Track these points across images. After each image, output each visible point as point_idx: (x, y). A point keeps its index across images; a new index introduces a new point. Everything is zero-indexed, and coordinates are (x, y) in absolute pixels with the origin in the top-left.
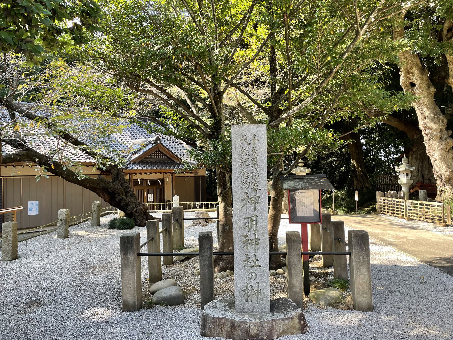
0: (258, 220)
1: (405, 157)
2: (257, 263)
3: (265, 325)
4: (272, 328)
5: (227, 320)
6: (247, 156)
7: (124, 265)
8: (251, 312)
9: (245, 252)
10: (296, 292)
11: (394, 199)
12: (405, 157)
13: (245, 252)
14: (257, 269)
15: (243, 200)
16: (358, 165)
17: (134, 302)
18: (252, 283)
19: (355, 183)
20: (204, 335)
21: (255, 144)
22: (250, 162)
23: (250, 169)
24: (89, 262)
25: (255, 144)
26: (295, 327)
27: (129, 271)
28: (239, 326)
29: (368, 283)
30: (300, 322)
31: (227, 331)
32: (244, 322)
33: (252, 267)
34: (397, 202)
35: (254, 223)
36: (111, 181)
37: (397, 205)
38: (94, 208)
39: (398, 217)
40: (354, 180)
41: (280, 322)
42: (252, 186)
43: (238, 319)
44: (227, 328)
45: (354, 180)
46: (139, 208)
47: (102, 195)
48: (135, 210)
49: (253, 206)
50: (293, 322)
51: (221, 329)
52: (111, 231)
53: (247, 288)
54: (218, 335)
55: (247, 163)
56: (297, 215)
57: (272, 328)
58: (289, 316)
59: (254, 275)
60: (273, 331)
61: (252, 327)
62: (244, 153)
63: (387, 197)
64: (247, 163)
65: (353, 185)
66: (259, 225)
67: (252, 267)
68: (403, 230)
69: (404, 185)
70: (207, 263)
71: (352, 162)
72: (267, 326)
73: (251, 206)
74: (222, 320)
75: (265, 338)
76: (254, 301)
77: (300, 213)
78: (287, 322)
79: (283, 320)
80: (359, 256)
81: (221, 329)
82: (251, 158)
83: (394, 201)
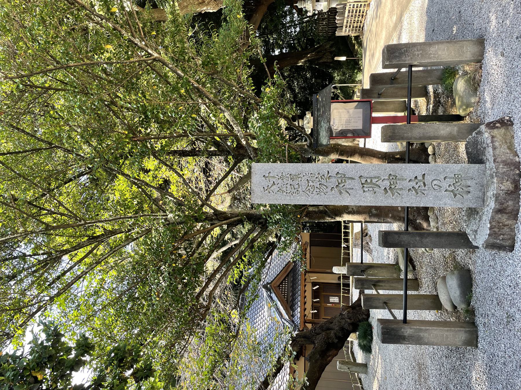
0: (366, 175)
1: (297, 5)
2: (420, 178)
3: (500, 170)
4: (505, 163)
5: (493, 218)
6: (288, 186)
7: (418, 341)
8: (483, 188)
9: (405, 192)
10: (458, 132)
11: (346, 15)
12: (297, 5)
13: (405, 192)
14: (428, 179)
15: (341, 193)
16: (304, 57)
17: (466, 332)
18: (445, 185)
19: (325, 61)
20: (512, 248)
21: (274, 177)
22: (295, 183)
23: (304, 183)
24: (412, 383)
25: (274, 177)
26: (505, 134)
27: (426, 335)
28: (502, 204)
29: (448, 45)
30: (497, 127)
31: (508, 219)
32: (497, 197)
33: (425, 185)
34: (349, 12)
35: (369, 181)
36: (313, 346)
37: (352, 12)
38: (345, 369)
39: (367, 11)
40: (321, 61)
41: (497, 152)
42: (323, 182)
43: (492, 204)
44: (504, 218)
45: (321, 61)
46: (346, 316)
47: (329, 358)
48: (348, 320)
49: (349, 182)
50: (498, 136)
51: (505, 226)
52: (373, 351)
53: (452, 191)
54: (513, 230)
55: (296, 186)
56: (361, 128)
57: (505, 163)
58: (489, 141)
59: (435, 182)
60: (509, 161)
61: (503, 187)
62: (284, 189)
63: (343, 23)
64: (296, 186)
65: (327, 62)
66: (372, 174)
67: (425, 185)
68: (383, 5)
69: (329, 4)
70: (418, 238)
71: (300, 64)
72: (502, 169)
73: (349, 184)
74: (494, 224)
75: (518, 172)
76: (469, 183)
77: (359, 125)
78: (497, 144)
79: (494, 148)
80: (414, 55)
81: (505, 226)
82: (290, 182)
83: (348, 16)
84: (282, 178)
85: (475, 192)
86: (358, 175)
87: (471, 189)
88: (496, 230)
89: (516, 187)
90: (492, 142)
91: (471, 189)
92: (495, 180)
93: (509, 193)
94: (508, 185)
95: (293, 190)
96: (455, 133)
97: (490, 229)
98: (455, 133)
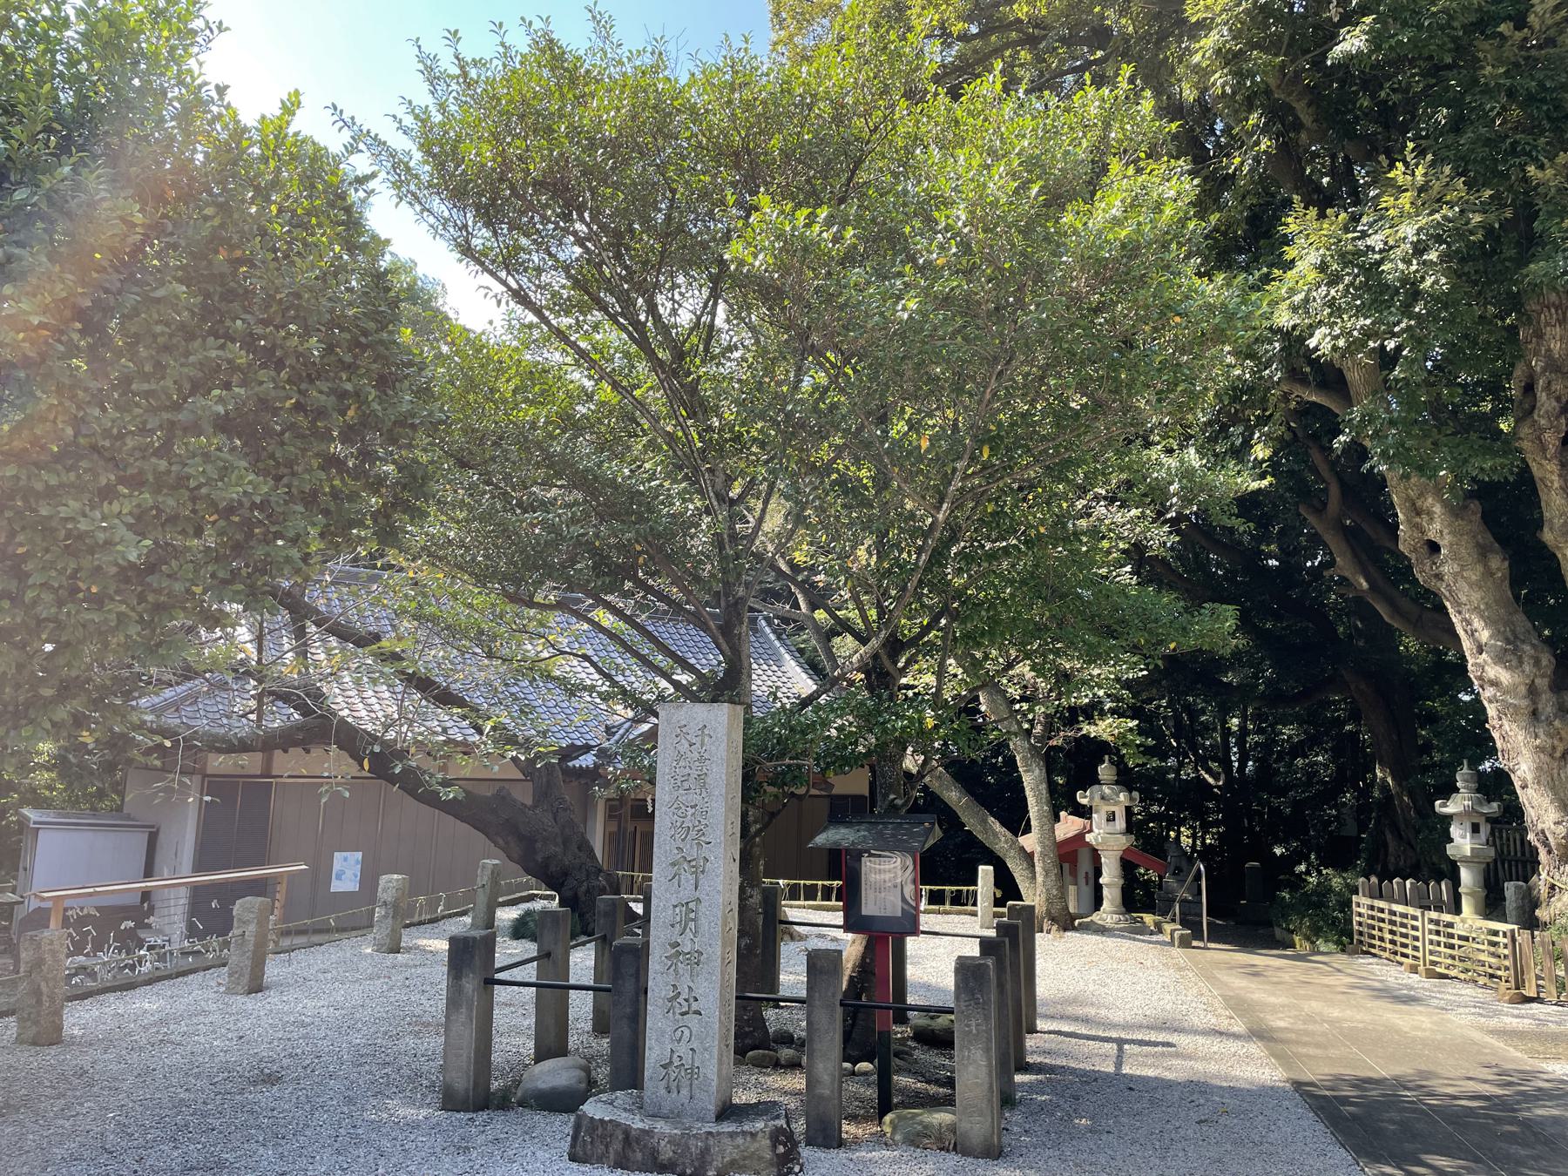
0: (702, 908)
1: (1465, 770)
2: (695, 1006)
3: (692, 1142)
4: (705, 1151)
5: (618, 1125)
6: (687, 770)
7: (453, 1003)
8: (672, 1116)
9: (671, 979)
10: (821, 1097)
11: (1395, 907)
12: (1465, 770)
13: (671, 979)
14: (692, 1020)
15: (673, 864)
16: (1400, 785)
17: (467, 1090)
18: (682, 1049)
19: (1391, 849)
20: (573, 1158)
21: (702, 745)
22: (691, 783)
23: (694, 798)
24: (418, 1011)
25: (702, 745)
26: (760, 1158)
27: (463, 1018)
28: (638, 1141)
29: (986, 1086)
30: (774, 1147)
31: (616, 1152)
32: (648, 1133)
33: (683, 1014)
34: (1405, 916)
35: (692, 915)
36: (529, 802)
37: (1404, 925)
38: (483, 878)
39: (1401, 964)
40: (1389, 836)
41: (727, 1141)
42: (693, 833)
43: (638, 1123)
44: (617, 1146)
45: (1389, 836)
46: (595, 883)
47: (501, 841)
48: (584, 888)
49: (692, 879)
50: (756, 1145)
51: (607, 1147)
52: (515, 943)
53: (671, 1062)
54: (600, 1160)
55: (686, 785)
56: (864, 912)
57: (705, 1151)
58: (746, 1128)
59: (687, 1032)
60: (709, 1159)
61: (663, 1143)
62: (682, 763)
63: (1392, 900)
64: (686, 785)
65: (1386, 855)
66: (703, 921)
67: (683, 1014)
68: (1404, 1007)
69: (1466, 860)
70: (628, 1010)
71: (1379, 774)
72: (695, 1146)
73: (687, 878)
74: (609, 1127)
75: (688, 1171)
76: (685, 1092)
77: (869, 908)
78: (740, 1140)
79: (732, 1135)
80: (968, 1017)
81: (607, 1147)
82: (694, 774)
83: (1393, 913)
84: (701, 759)
85: (669, 1101)
86: (702, 897)
87: (674, 1095)
88: (600, 1131)
89: (662, 1168)
90: (744, 1133)
91: (674, 1095)
92: (678, 1132)
93: (654, 1153)
94: (667, 1152)
95: (680, 779)
96: (819, 1091)
97: (601, 1121)
98: (819, 1091)
